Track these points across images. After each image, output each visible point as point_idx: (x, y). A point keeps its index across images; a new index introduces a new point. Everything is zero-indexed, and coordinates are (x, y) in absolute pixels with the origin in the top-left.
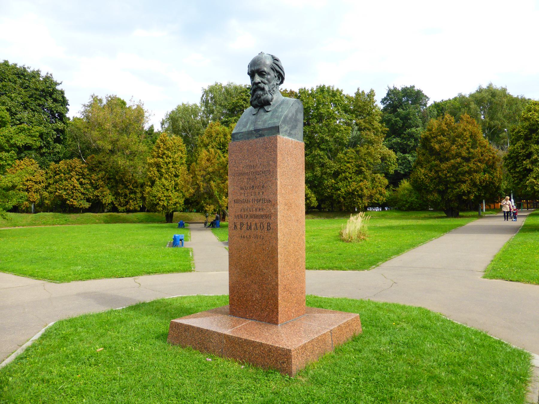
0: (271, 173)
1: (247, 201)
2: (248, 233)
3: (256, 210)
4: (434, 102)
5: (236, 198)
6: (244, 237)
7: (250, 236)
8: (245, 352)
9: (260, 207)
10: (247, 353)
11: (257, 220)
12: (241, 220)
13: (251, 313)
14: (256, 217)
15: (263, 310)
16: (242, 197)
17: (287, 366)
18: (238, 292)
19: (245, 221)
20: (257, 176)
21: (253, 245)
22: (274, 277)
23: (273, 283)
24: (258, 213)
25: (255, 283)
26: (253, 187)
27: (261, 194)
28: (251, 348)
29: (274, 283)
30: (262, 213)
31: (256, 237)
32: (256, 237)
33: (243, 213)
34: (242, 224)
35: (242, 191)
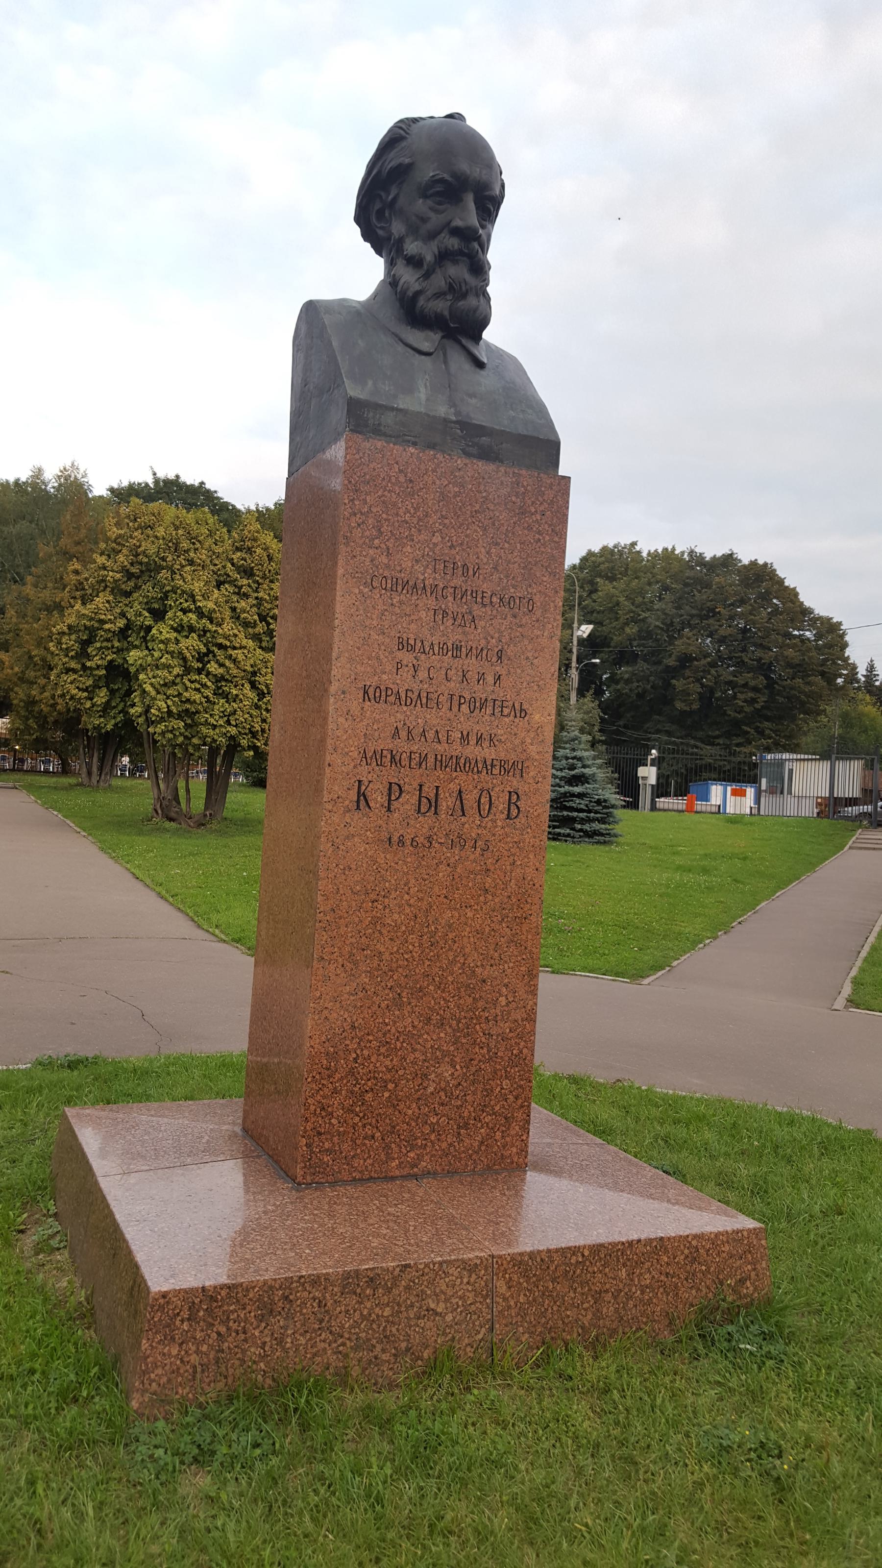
0: (539, 613)
1: (425, 700)
2: (423, 825)
3: (465, 738)
4: (178, 477)
5: (374, 681)
6: (401, 842)
7: (429, 839)
8: (598, 1297)
9: (484, 729)
10: (608, 1297)
11: (462, 779)
12: (391, 774)
13: (413, 1147)
14: (460, 764)
15: (466, 1126)
16: (405, 681)
17: (755, 1289)
18: (352, 1072)
19: (410, 779)
20: (477, 611)
21: (443, 872)
22: (521, 993)
23: (513, 1016)
24: (472, 751)
25: (441, 1025)
26: (459, 648)
27: (490, 679)
28: (623, 1273)
29: (518, 1015)
30: (488, 753)
31: (459, 841)
32: (459, 841)
33: (402, 746)
34: (394, 790)
35: (407, 658)
